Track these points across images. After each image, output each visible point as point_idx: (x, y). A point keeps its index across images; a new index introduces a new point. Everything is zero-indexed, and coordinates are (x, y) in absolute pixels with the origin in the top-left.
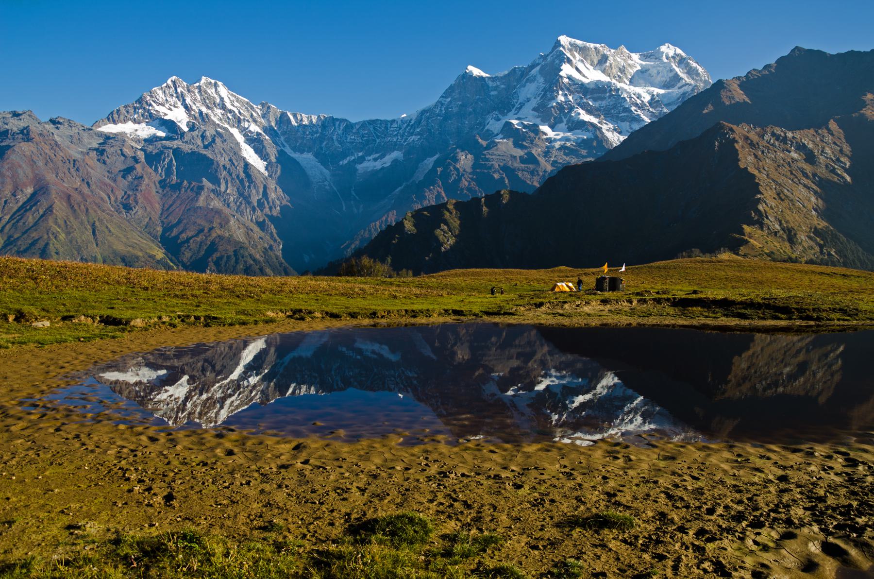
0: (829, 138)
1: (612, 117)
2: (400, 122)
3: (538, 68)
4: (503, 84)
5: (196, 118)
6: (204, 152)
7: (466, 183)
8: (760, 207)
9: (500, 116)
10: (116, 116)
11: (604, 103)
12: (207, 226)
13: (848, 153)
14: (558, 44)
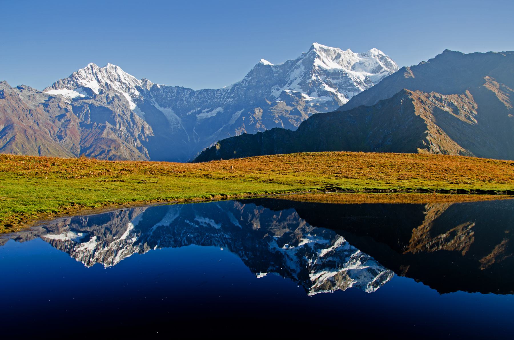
0: (466, 100)
1: (344, 89)
2: (222, 91)
3: (301, 61)
4: (281, 69)
5: (103, 87)
6: (107, 106)
7: (259, 126)
8: (428, 138)
9: (279, 88)
10: (57, 85)
11: (338, 81)
12: (107, 149)
14: (313, 47)
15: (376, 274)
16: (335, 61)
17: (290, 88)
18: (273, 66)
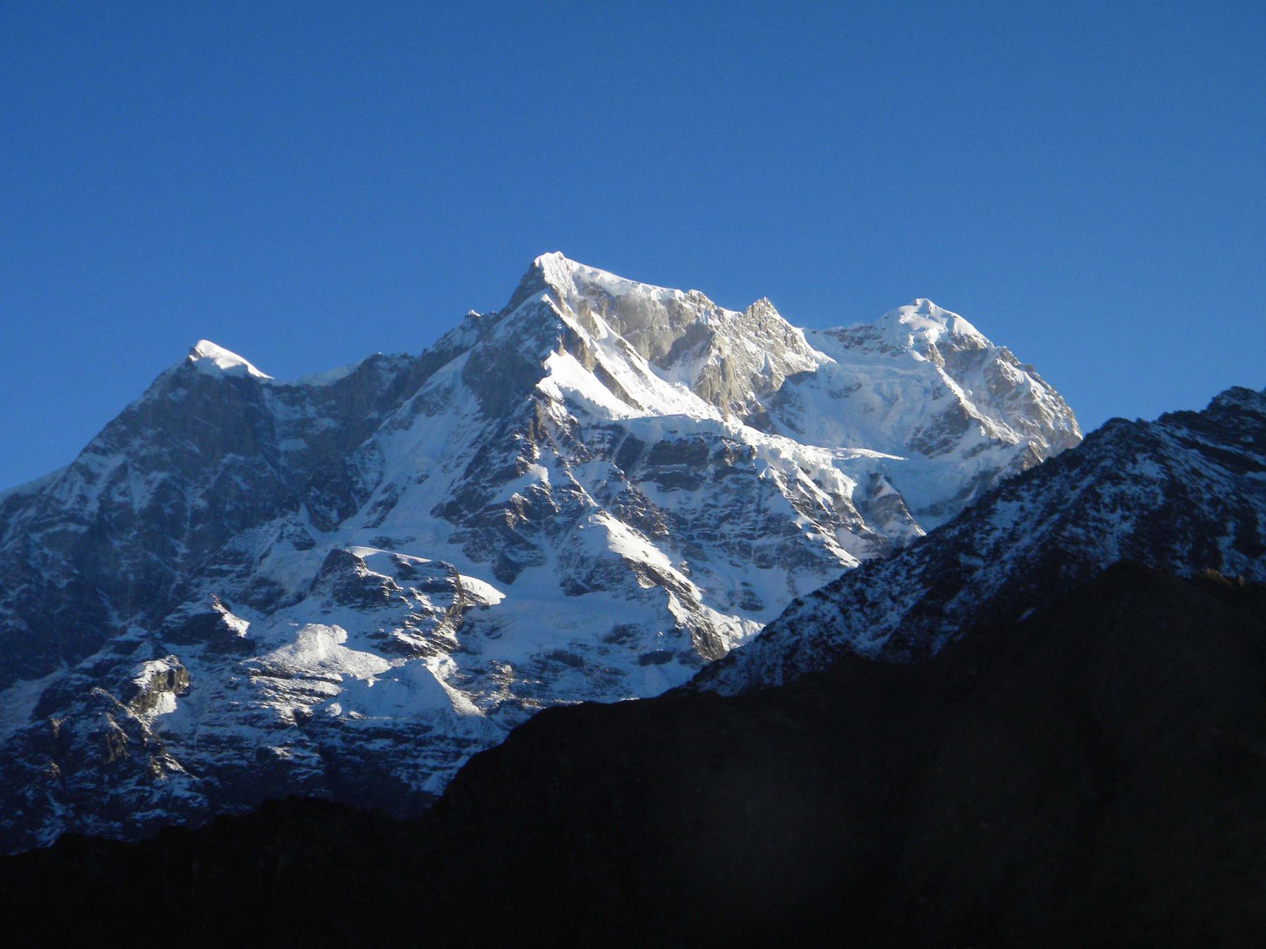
3: (460, 362)
14: (535, 280)
16: (677, 369)
17: (383, 532)
18: (277, 390)
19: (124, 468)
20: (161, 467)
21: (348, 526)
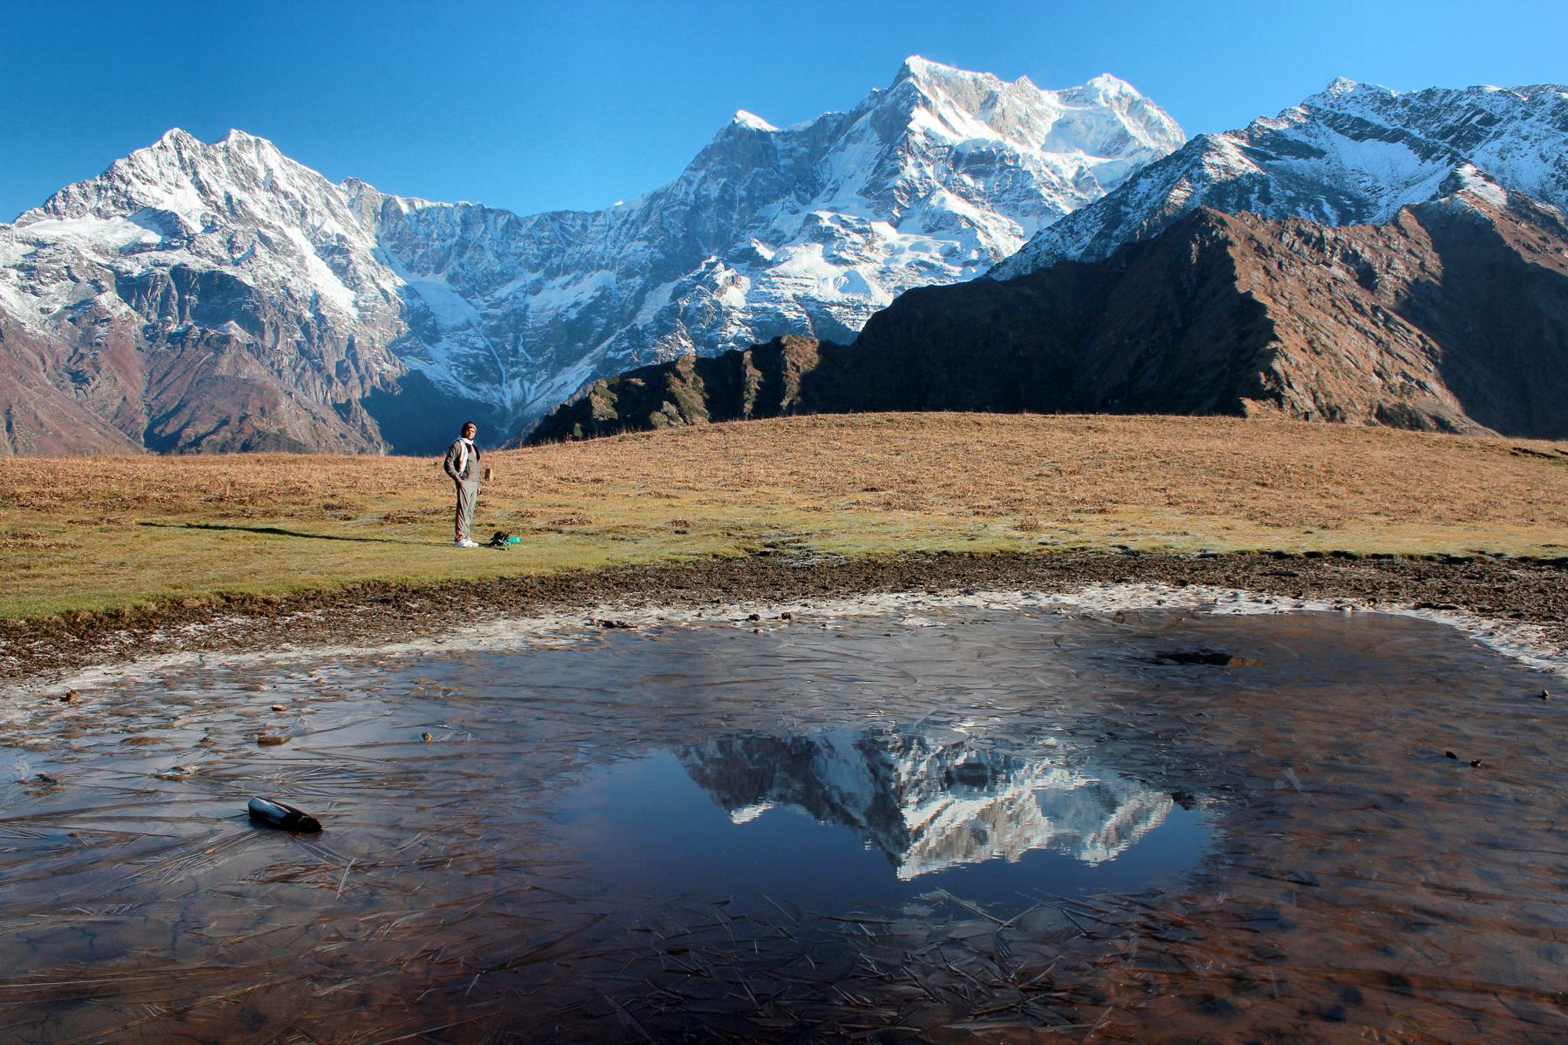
0: (1399, 243)
3: (869, 115)
5: (218, 208)
6: (228, 270)
8: (1277, 366)
12: (236, 414)
13: (1434, 270)
14: (905, 71)
15: (1112, 805)
19: (705, 178)
20: (722, 176)
21: (815, 201)
